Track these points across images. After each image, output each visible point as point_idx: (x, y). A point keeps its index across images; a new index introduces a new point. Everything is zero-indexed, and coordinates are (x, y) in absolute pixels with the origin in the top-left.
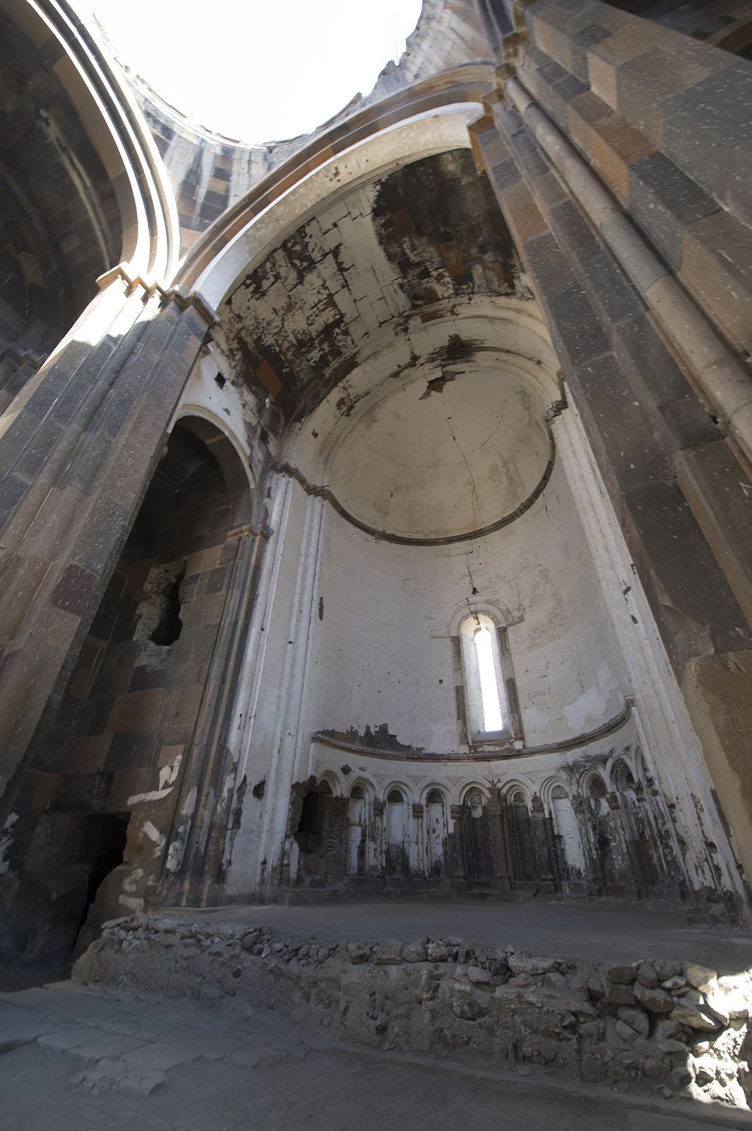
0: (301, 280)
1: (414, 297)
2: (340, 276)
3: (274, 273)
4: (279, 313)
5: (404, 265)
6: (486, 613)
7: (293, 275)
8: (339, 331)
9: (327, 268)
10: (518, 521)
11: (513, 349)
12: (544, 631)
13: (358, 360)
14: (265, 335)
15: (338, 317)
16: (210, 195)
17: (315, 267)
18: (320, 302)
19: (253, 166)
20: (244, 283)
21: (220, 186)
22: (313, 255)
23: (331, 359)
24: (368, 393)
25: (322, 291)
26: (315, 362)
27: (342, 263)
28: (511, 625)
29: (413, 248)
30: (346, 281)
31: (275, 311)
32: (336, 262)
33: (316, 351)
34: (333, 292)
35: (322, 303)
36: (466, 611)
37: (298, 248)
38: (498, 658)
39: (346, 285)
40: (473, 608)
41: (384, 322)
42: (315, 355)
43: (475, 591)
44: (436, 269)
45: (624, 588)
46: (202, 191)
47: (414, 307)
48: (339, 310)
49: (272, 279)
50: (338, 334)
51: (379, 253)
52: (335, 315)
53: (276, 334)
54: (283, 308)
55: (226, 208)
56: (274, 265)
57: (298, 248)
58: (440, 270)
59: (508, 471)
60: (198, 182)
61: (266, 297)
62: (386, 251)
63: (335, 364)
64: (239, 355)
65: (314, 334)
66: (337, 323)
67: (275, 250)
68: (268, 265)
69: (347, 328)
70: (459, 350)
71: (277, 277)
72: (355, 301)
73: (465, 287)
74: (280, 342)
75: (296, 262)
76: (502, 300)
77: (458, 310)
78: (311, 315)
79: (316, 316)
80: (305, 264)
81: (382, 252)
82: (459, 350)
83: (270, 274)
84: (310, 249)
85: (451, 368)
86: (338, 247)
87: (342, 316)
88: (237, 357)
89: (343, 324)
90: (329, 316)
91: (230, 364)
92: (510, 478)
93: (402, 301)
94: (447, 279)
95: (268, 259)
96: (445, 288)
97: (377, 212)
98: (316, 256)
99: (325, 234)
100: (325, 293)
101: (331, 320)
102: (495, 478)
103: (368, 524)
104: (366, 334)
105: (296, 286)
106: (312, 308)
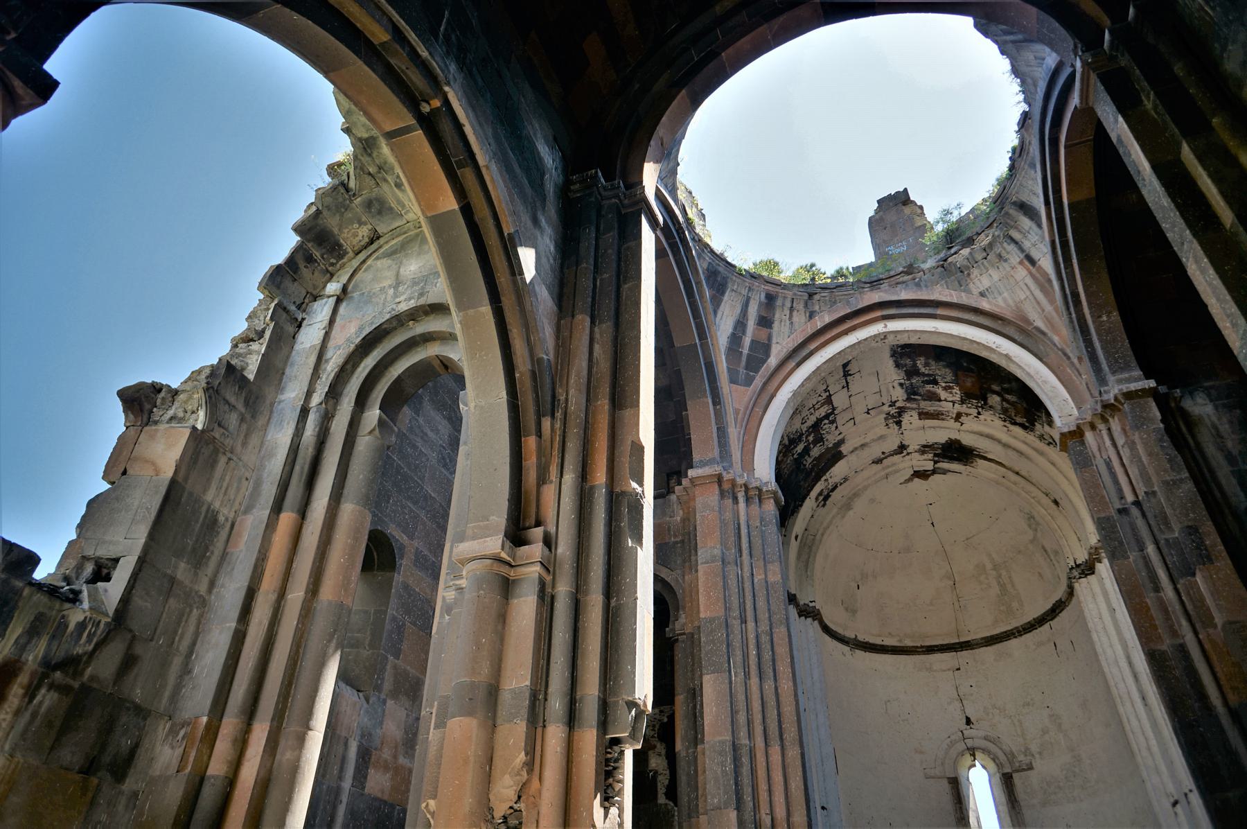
1: (912, 393)
5: (912, 372)
6: (984, 751)
10: (1014, 643)
11: (1023, 473)
12: (1060, 788)
13: (844, 449)
16: (754, 343)
19: (795, 313)
21: (762, 336)
24: (846, 479)
28: (1017, 771)
29: (926, 365)
36: (961, 746)
38: (1004, 809)
40: (970, 743)
42: (800, 448)
43: (968, 721)
45: (1172, 800)
46: (747, 341)
47: (908, 399)
59: (1000, 576)
60: (744, 332)
62: (895, 362)
63: (816, 451)
66: (827, 416)
70: (956, 452)
76: (1017, 430)
77: (963, 419)
82: (956, 452)
85: (944, 465)
87: (834, 409)
90: (822, 412)
92: (1002, 586)
93: (899, 394)
94: (956, 390)
100: (825, 395)
102: (982, 578)
103: (840, 631)
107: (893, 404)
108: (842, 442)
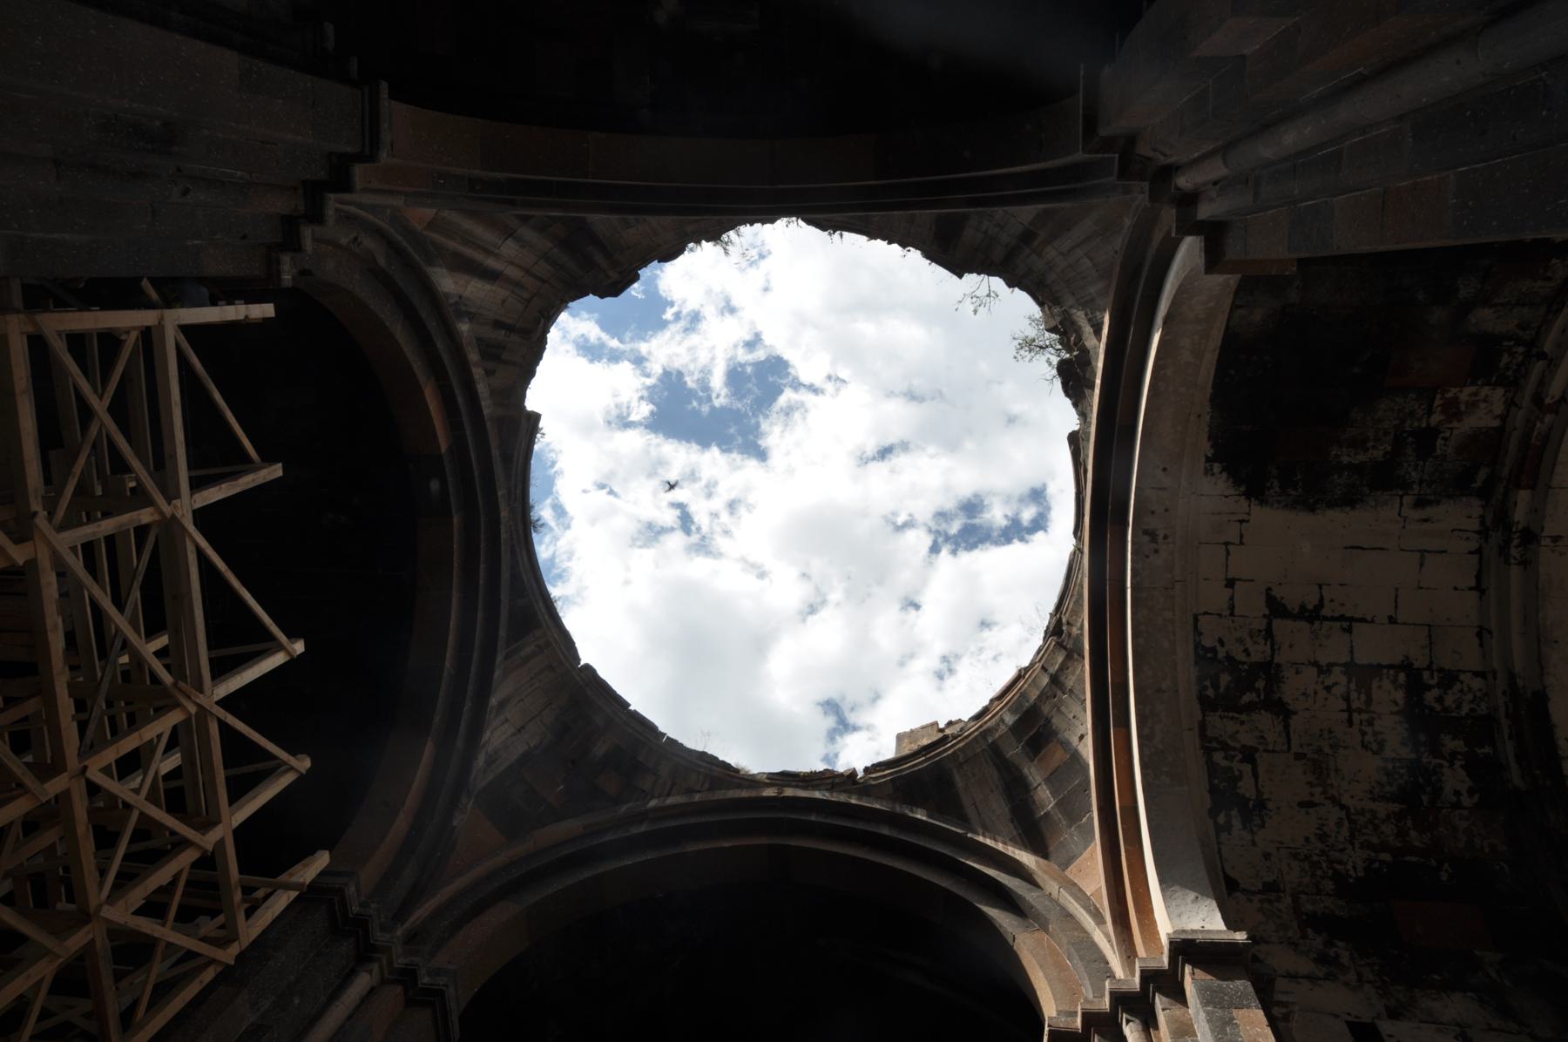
0: (1282, 711)
1: (1460, 485)
2: (1327, 624)
3: (1240, 756)
4: (1316, 800)
5: (1383, 478)
7: (1265, 721)
8: (1436, 692)
9: (1295, 640)
14: (1340, 862)
15: (1402, 677)
17: (1279, 665)
18: (1347, 699)
20: (1219, 829)
22: (1256, 657)
23: (1487, 750)
25: (1328, 682)
26: (1471, 792)
27: (1303, 607)
30: (1342, 618)
31: (1307, 805)
32: (1295, 617)
33: (1446, 771)
34: (1345, 659)
35: (1354, 695)
37: (1225, 679)
39: (1348, 623)
41: (1478, 577)
42: (1455, 780)
44: (1430, 412)
48: (1390, 667)
49: (1247, 768)
50: (1440, 700)
51: (1334, 520)
52: (1394, 681)
53: (1352, 836)
54: (1310, 784)
55: (1086, 768)
56: (1225, 747)
57: (1225, 679)
58: (1438, 402)
61: (1270, 805)
62: (1332, 505)
64: (1342, 951)
65: (1406, 753)
67: (1203, 727)
68: (1218, 757)
69: (1441, 670)
71: (1249, 756)
72: (1392, 620)
73: (1505, 359)
74: (1375, 840)
75: (1247, 698)
78: (1364, 734)
79: (1370, 723)
80: (1260, 684)
81: (1331, 513)
83: (1236, 765)
84: (1241, 657)
86: (1271, 600)
87: (1406, 666)
88: (1345, 958)
89: (1426, 674)
90: (1388, 694)
91: (1347, 984)
93: (1458, 517)
94: (1465, 394)
95: (1208, 751)
96: (1482, 405)
97: (1254, 490)
98: (1259, 651)
99: (1232, 614)
100: (1337, 675)
101: (1400, 696)
104: (1479, 635)
105: (1287, 727)
106: (1350, 723)
107: (1484, 532)
108: (1512, 677)
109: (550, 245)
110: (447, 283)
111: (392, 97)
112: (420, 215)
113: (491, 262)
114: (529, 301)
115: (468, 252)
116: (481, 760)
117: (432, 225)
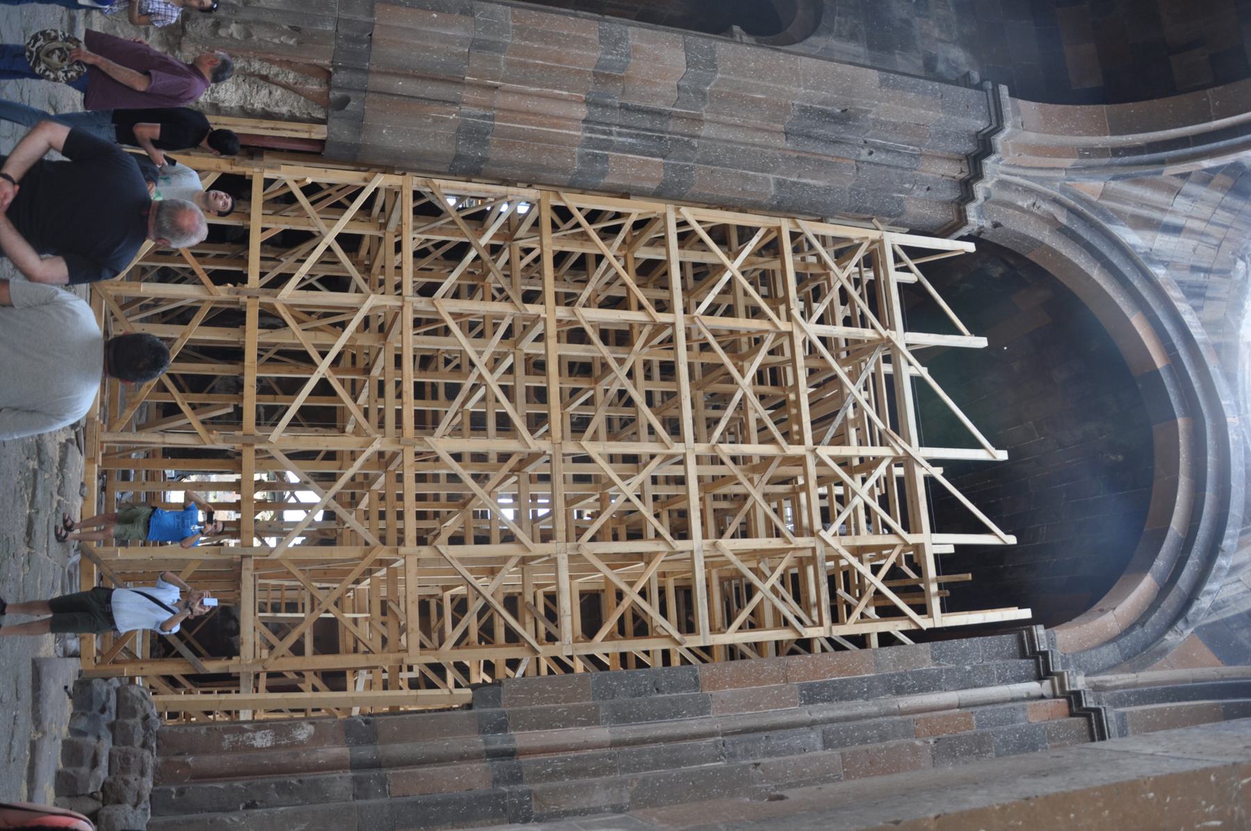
109: (1221, 195)
110: (1130, 237)
111: (1011, 95)
112: (1091, 187)
113: (1168, 219)
114: (1219, 246)
115: (1145, 212)
116: (1204, 602)
117: (1104, 195)
